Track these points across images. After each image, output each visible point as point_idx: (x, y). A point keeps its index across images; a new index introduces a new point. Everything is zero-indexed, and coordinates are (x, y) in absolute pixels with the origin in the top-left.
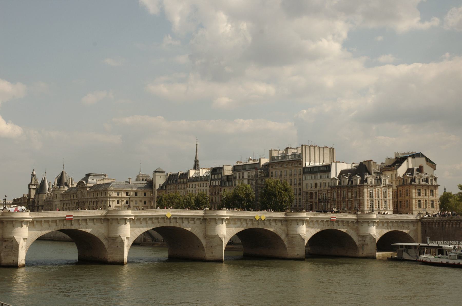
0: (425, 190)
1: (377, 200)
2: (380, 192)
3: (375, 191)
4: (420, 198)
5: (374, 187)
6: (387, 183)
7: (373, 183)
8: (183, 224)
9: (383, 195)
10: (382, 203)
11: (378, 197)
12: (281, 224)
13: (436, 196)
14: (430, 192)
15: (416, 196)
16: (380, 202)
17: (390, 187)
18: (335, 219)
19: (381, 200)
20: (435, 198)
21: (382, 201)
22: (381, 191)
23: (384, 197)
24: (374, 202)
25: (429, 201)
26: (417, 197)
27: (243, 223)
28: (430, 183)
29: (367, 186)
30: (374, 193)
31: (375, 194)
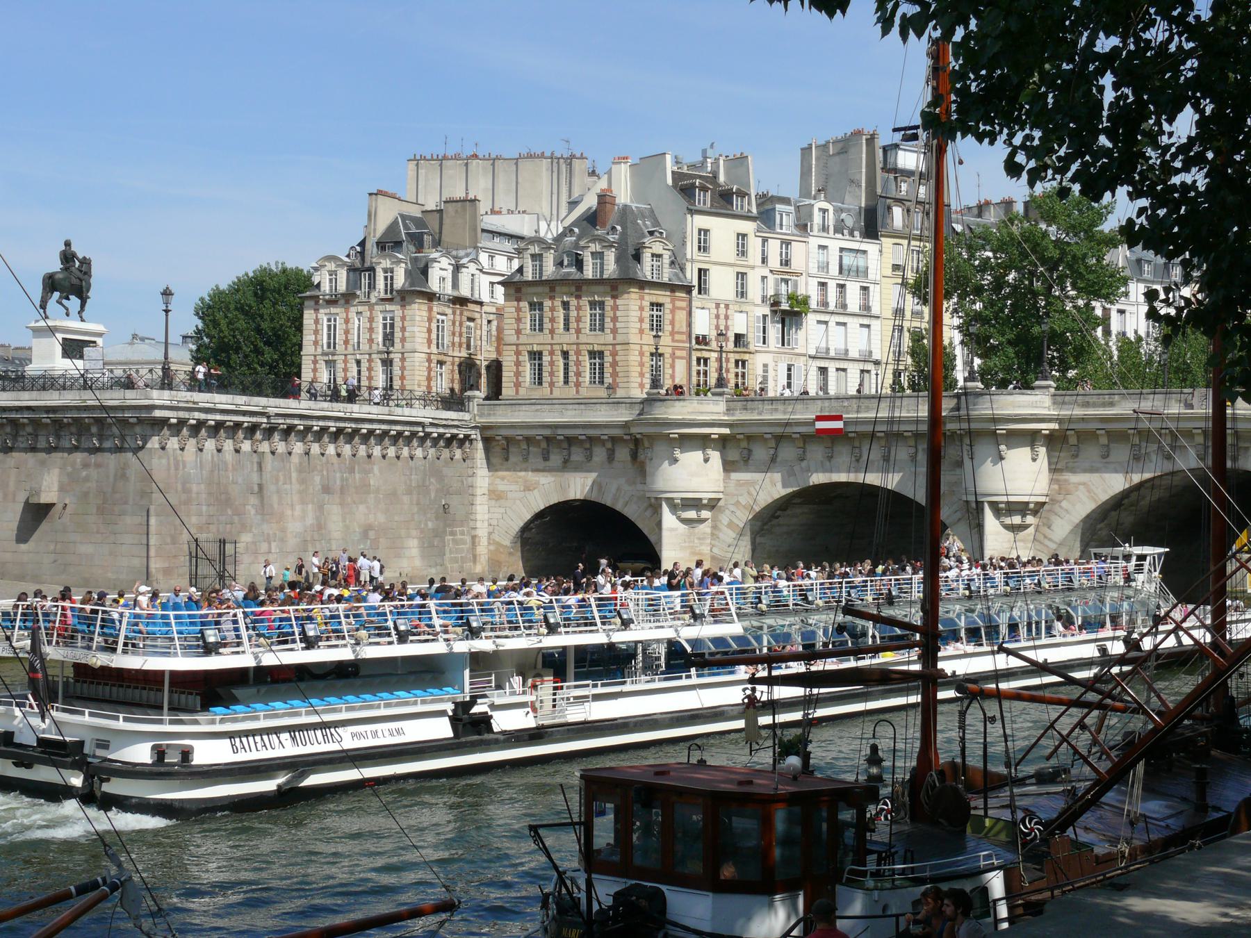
0: (566, 305)
1: (349, 357)
4: (538, 341)
5: (342, 302)
6: (400, 281)
7: (342, 287)
13: (614, 331)
14: (587, 311)
15: (518, 332)
16: (364, 365)
17: (407, 300)
19: (367, 356)
20: (609, 338)
21: (370, 361)
24: (340, 365)
25: (578, 353)
26: (523, 339)
28: (589, 273)
31: (347, 332)
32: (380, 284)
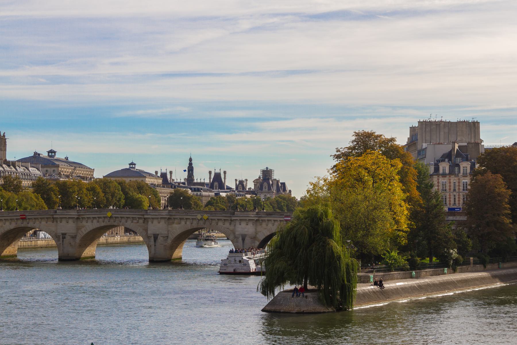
2: (457, 184)
3: (450, 183)
7: (447, 171)
8: (127, 223)
9: (461, 188)
10: (459, 198)
11: (455, 190)
12: (229, 224)
18: (290, 218)
21: (459, 195)
22: (459, 182)
23: (464, 190)
27: (188, 223)
29: (438, 177)
30: (448, 185)
31: (450, 186)
32: (462, 171)
